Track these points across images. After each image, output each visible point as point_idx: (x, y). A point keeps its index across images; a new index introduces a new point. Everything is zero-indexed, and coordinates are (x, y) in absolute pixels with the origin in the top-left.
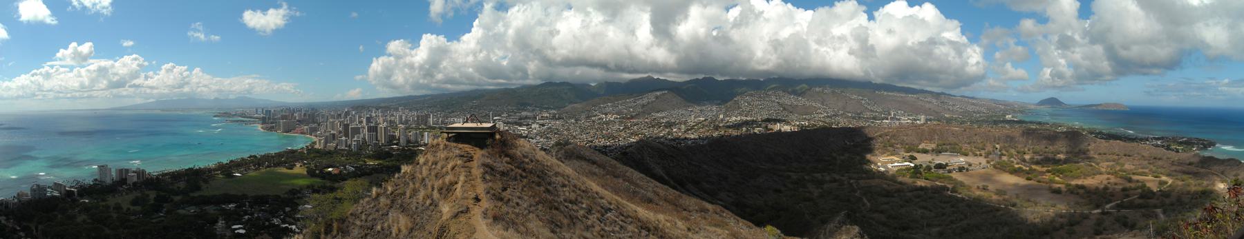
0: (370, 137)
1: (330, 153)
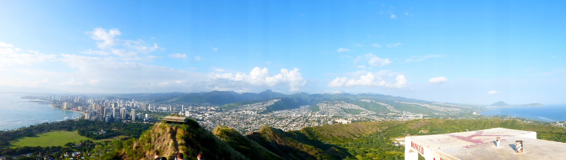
1: (92, 122)
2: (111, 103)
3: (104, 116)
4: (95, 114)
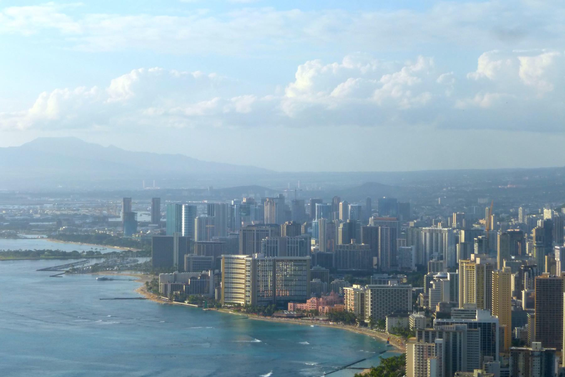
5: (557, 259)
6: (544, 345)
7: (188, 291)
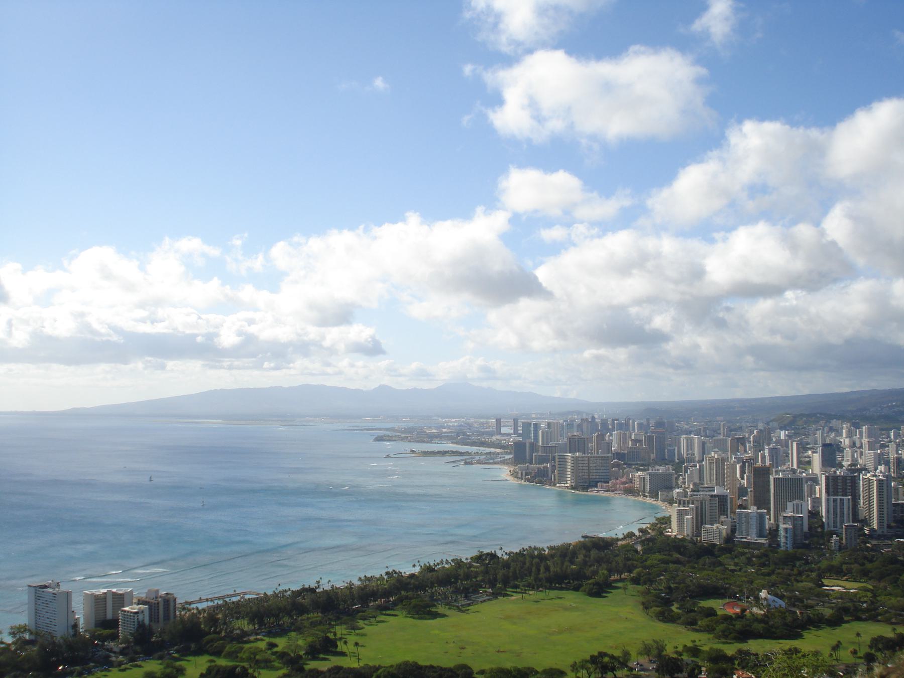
0: (834, 509)
1: (709, 550)
2: (803, 448)
3: (769, 522)
4: (723, 510)
5: (767, 454)
6: (758, 509)
7: (536, 476)
